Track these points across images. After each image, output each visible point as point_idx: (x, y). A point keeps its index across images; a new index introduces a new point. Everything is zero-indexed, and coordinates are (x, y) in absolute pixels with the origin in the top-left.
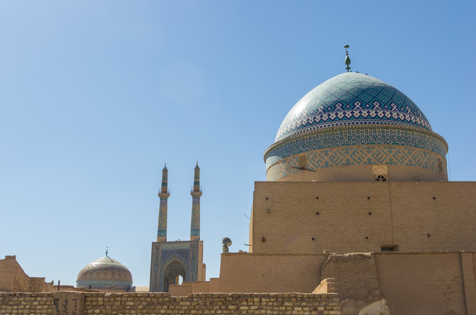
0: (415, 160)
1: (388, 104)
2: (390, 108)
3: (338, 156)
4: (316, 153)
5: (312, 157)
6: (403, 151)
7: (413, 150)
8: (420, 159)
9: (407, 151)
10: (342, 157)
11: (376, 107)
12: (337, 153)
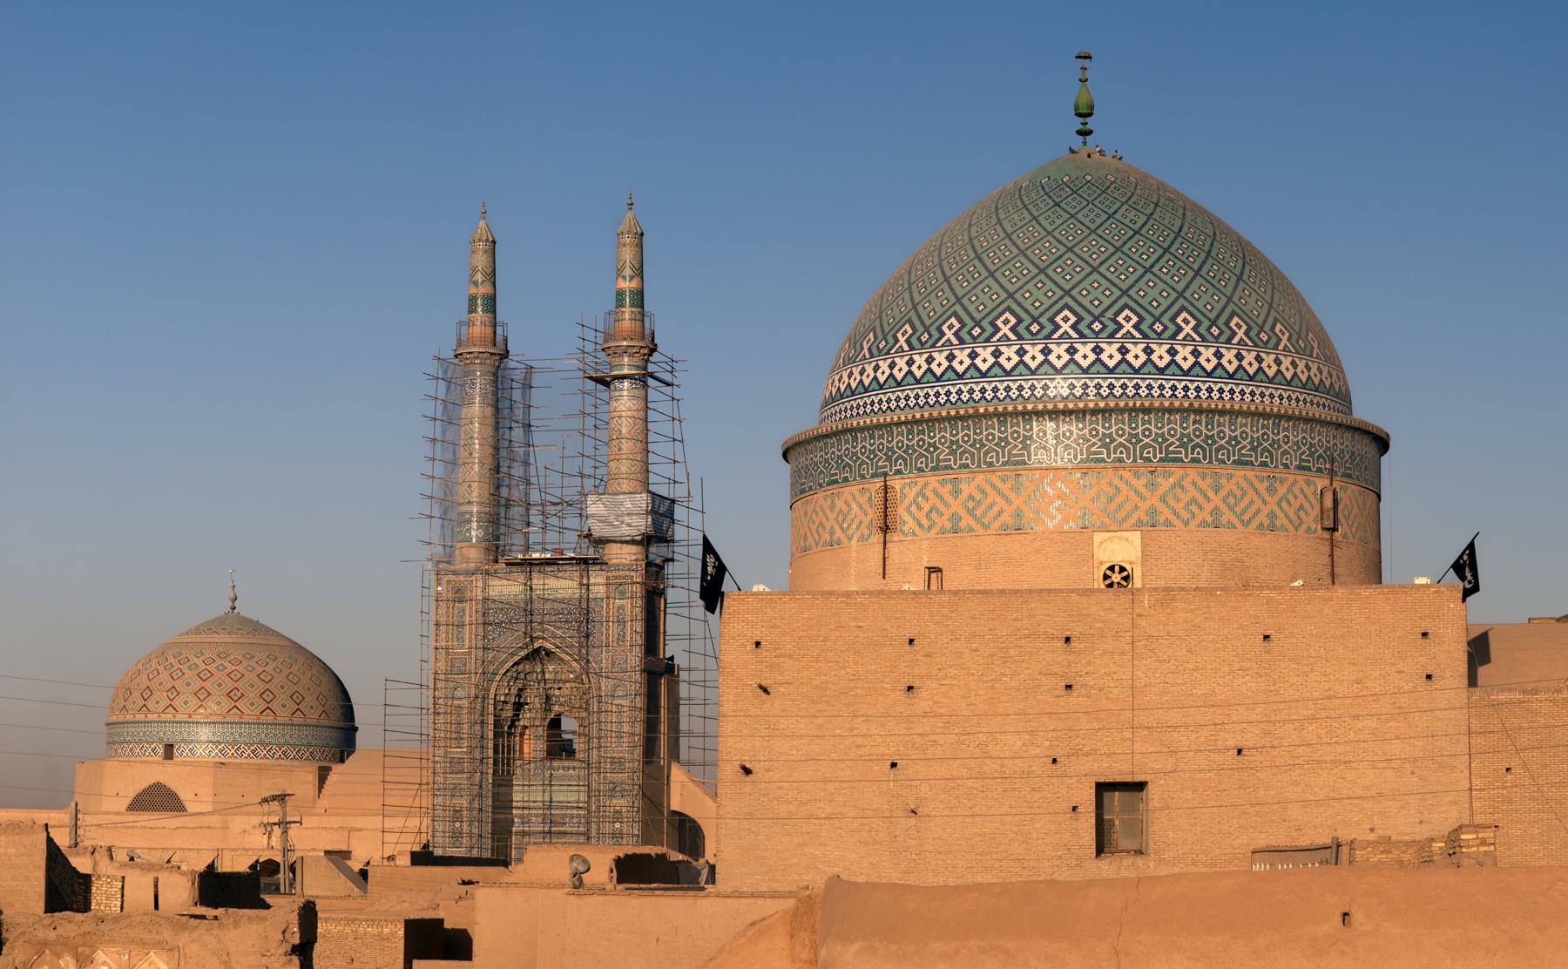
0: (1231, 508)
1: (1165, 320)
2: (1172, 328)
3: (990, 500)
4: (926, 484)
5: (912, 494)
6: (1194, 484)
7: (1230, 476)
8: (1252, 502)
9: (1208, 481)
10: (1001, 503)
11: (1123, 331)
12: (988, 489)
